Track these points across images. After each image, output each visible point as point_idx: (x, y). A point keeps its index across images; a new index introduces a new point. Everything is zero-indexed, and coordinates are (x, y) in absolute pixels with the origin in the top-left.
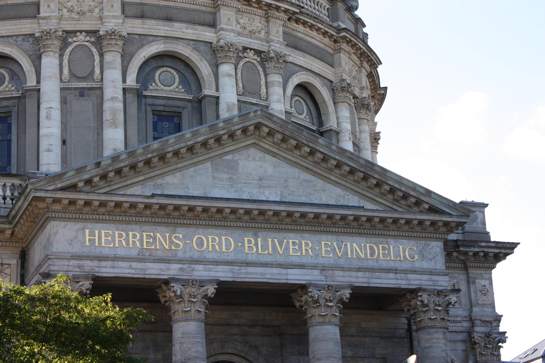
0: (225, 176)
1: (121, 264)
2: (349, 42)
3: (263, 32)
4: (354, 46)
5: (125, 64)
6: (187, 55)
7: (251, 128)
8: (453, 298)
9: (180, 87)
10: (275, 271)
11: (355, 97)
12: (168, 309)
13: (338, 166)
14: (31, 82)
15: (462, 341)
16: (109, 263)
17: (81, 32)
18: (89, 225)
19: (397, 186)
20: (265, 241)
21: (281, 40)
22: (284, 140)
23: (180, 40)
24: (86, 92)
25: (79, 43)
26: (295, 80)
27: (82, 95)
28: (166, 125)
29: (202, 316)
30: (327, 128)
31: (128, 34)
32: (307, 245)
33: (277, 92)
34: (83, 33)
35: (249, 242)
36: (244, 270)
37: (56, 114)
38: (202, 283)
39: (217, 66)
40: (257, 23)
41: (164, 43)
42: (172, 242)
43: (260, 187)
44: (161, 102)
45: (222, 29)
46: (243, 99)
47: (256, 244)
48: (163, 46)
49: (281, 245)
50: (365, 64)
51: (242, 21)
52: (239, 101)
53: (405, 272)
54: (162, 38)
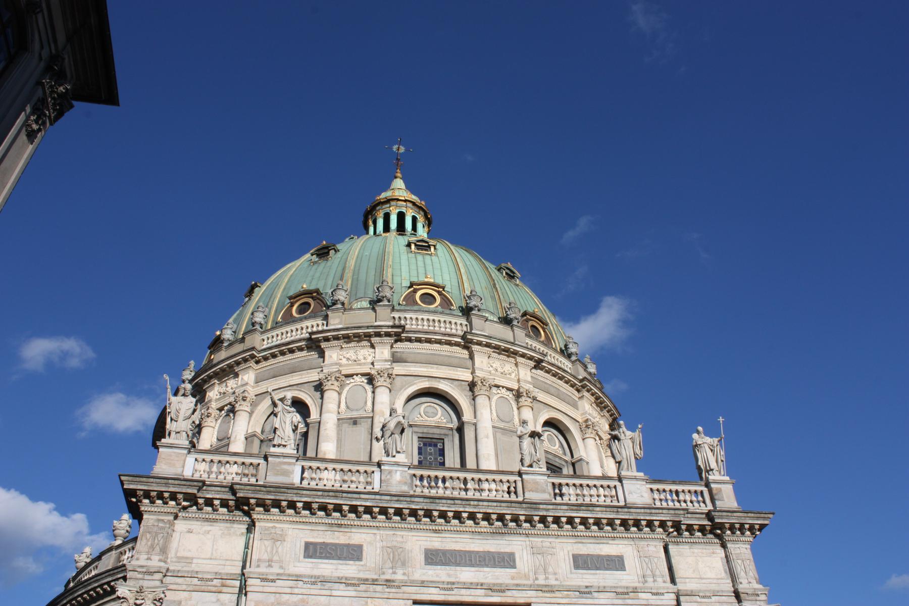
2: (588, 391)
3: (513, 375)
9: (442, 418)
14: (314, 415)
17: (357, 375)
23: (442, 381)
25: (355, 383)
27: (355, 423)
28: (430, 450)
30: (577, 458)
31: (396, 375)
34: (359, 375)
39: (474, 399)
41: (428, 381)
48: (427, 383)
51: (494, 365)
54: (427, 379)
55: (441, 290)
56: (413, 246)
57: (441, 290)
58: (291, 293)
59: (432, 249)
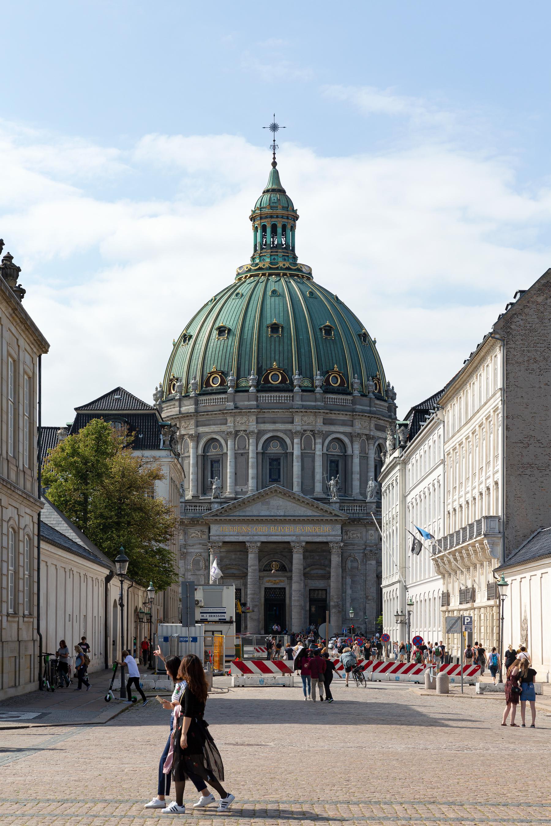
0: (266, 506)
1: (231, 537)
2: (359, 415)
3: (314, 422)
4: (362, 416)
5: (268, 431)
6: (281, 436)
7: (273, 492)
8: (342, 544)
10: (280, 537)
11: (366, 435)
12: (248, 549)
13: (303, 502)
14: (225, 451)
15: (363, 553)
16: (228, 537)
18: (222, 525)
19: (322, 508)
20: (278, 527)
21: (322, 424)
22: (284, 494)
24: (243, 454)
26: (330, 438)
29: (257, 552)
32: (292, 528)
33: (319, 447)
35: (272, 528)
36: (270, 537)
37: (233, 464)
38: (256, 542)
40: (312, 418)
42: (247, 529)
43: (278, 509)
44: (273, 455)
45: (295, 425)
46: (304, 451)
47: (275, 529)
49: (283, 529)
50: (372, 419)
52: (301, 453)
53: (326, 536)
55: (282, 371)
56: (269, 329)
57: (282, 371)
58: (207, 371)
59: (280, 329)
